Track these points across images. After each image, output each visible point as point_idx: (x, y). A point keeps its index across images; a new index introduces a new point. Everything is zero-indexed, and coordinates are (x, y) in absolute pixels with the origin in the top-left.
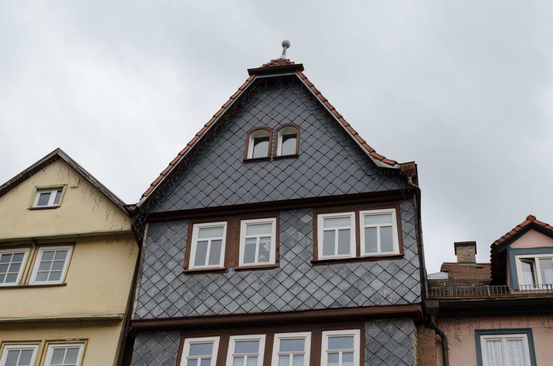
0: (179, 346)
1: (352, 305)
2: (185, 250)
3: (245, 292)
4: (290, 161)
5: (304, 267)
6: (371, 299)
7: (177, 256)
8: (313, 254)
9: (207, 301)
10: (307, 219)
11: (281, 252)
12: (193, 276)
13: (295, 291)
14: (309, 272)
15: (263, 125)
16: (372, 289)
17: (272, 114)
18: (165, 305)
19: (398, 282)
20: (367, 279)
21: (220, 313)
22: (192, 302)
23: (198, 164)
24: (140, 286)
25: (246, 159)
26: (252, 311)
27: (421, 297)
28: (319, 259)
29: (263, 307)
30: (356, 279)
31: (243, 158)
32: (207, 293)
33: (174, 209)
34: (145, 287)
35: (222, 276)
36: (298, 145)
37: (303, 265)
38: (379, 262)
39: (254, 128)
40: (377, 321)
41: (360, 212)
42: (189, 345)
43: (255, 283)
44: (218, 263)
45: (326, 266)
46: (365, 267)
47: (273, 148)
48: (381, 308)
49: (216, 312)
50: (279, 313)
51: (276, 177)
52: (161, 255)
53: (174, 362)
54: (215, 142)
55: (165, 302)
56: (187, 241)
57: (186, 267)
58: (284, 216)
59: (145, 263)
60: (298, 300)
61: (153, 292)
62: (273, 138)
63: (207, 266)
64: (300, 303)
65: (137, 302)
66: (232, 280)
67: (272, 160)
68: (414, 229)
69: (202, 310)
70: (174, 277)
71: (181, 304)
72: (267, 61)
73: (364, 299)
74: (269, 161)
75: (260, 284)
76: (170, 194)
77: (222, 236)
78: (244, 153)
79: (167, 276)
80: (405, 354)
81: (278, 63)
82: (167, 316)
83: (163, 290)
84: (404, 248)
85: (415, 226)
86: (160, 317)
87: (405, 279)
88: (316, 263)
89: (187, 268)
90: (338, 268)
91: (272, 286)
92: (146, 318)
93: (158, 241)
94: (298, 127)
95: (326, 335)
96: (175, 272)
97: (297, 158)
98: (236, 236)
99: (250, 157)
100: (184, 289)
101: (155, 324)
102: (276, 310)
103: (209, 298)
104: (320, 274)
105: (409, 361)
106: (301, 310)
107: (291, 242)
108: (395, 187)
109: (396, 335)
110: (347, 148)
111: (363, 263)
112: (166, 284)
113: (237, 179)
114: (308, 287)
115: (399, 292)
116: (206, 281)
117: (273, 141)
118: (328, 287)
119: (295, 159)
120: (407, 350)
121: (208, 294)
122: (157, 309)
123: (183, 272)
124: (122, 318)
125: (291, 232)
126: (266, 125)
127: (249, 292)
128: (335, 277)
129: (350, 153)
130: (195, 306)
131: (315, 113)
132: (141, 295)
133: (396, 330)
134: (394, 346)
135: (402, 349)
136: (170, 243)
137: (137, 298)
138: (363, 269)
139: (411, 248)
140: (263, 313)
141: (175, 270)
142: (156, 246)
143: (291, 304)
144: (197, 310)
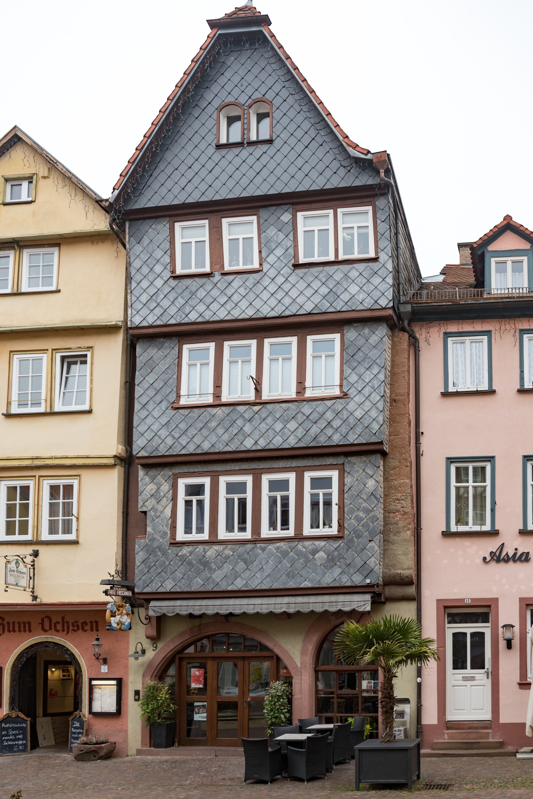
0: (178, 353)
1: (331, 310)
2: (169, 252)
3: (232, 297)
4: (264, 147)
5: (287, 271)
6: (349, 304)
7: (162, 259)
8: (294, 257)
9: (197, 306)
10: (286, 217)
11: (264, 255)
12: (181, 280)
13: (280, 295)
14: (291, 276)
15: (233, 100)
16: (349, 293)
17: (242, 85)
18: (158, 311)
19: (373, 286)
20: (344, 283)
21: (211, 319)
22: (183, 308)
23: (168, 150)
24: (131, 292)
25: (218, 144)
26: (240, 317)
27: (392, 301)
28: (300, 262)
29: (250, 313)
30: (334, 283)
31: (215, 142)
32: (197, 299)
33: (150, 205)
34: (136, 293)
35: (209, 280)
36: (272, 127)
37: (285, 269)
38: (355, 265)
39: (223, 103)
40: (355, 325)
41: (338, 209)
42: (188, 351)
43: (241, 288)
44: (205, 267)
45: (307, 270)
46: (343, 270)
47: (246, 130)
48: (357, 313)
49: (207, 318)
50: (265, 318)
51: (251, 167)
52: (147, 258)
53: (175, 368)
54: (184, 122)
55: (158, 309)
56: (170, 242)
57: (173, 271)
58: (264, 213)
59: (132, 267)
60: (282, 305)
61: (144, 298)
62: (245, 117)
63: (193, 270)
64: (284, 308)
65: (131, 308)
66: (218, 285)
67: (246, 145)
68: (389, 230)
69: (193, 317)
70: (163, 282)
71: (172, 310)
72: (230, 9)
73: (342, 304)
74: (242, 146)
75: (246, 289)
76: (144, 186)
77: (205, 236)
78: (215, 136)
79: (155, 281)
80: (378, 356)
81: (243, 12)
82: (162, 323)
83: (154, 296)
84: (379, 251)
85: (389, 227)
86: (155, 324)
87: (379, 283)
88: (297, 266)
89: (174, 272)
90: (318, 272)
91: (258, 291)
92: (141, 325)
93: (141, 242)
94: (271, 103)
95: (310, 339)
96: (163, 277)
97: (272, 144)
98: (218, 237)
99: (223, 140)
100: (174, 294)
101: (151, 331)
102: (262, 316)
103: (199, 304)
104: (301, 278)
105: (381, 363)
106: (285, 315)
107: (272, 244)
108: (370, 181)
109: (371, 338)
110: (322, 133)
111: (341, 267)
112: (156, 290)
113: (212, 168)
114: (290, 291)
115: (373, 297)
116: (194, 286)
117: (246, 121)
118: (309, 292)
119: (270, 145)
120: (380, 353)
121: (198, 300)
122: (151, 315)
123: (171, 276)
124: (122, 326)
125: (272, 232)
126: (237, 99)
127: (236, 298)
128: (315, 281)
129: (325, 138)
130: (187, 312)
131: (287, 84)
132: (133, 300)
133: (372, 334)
134: (369, 349)
135: (375, 351)
136: (154, 244)
137: (130, 305)
138: (341, 273)
139: (386, 250)
140: (251, 319)
141: (162, 274)
142: (140, 248)
143: (276, 309)
144: (189, 316)
